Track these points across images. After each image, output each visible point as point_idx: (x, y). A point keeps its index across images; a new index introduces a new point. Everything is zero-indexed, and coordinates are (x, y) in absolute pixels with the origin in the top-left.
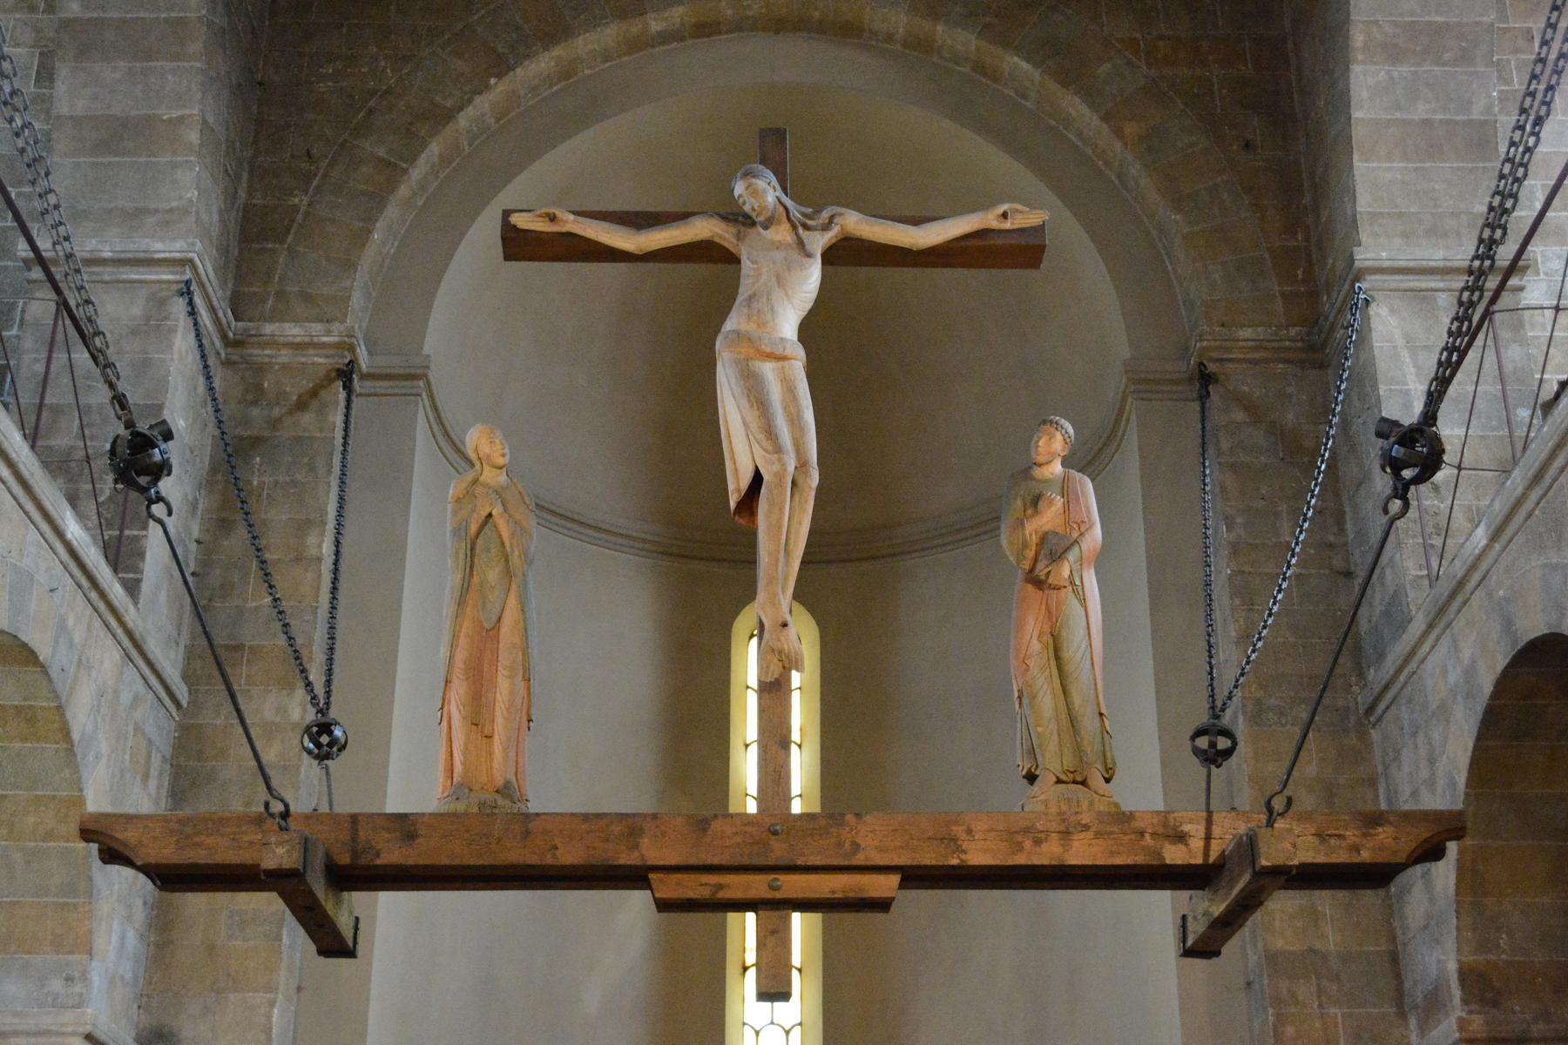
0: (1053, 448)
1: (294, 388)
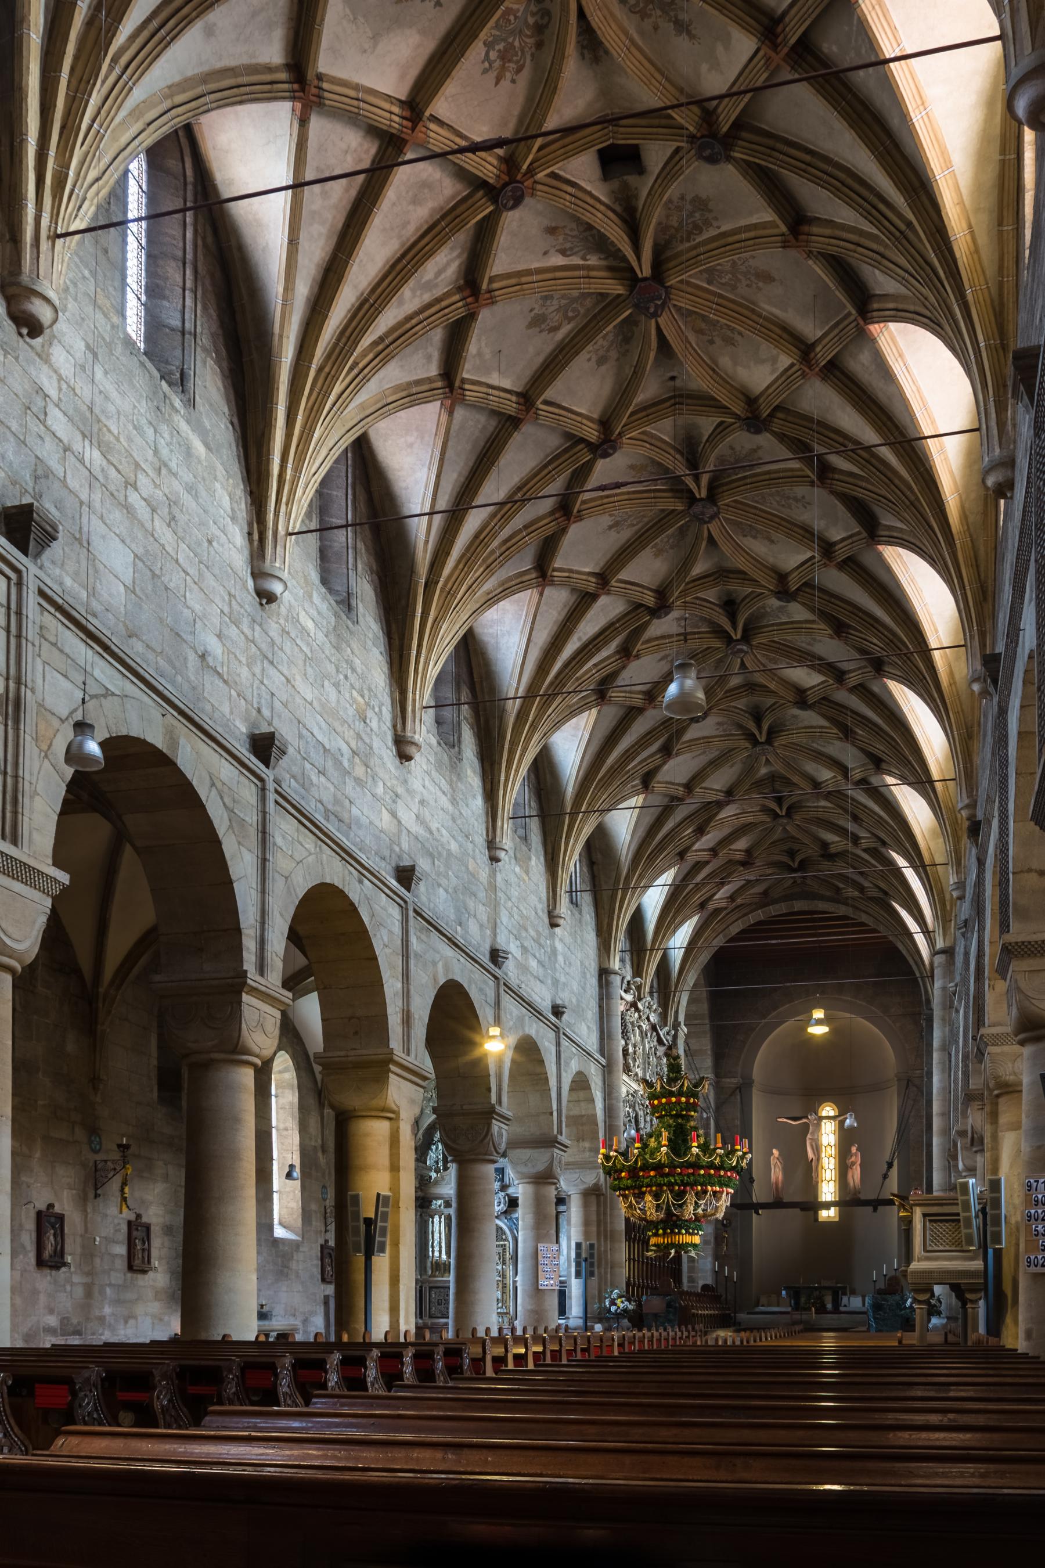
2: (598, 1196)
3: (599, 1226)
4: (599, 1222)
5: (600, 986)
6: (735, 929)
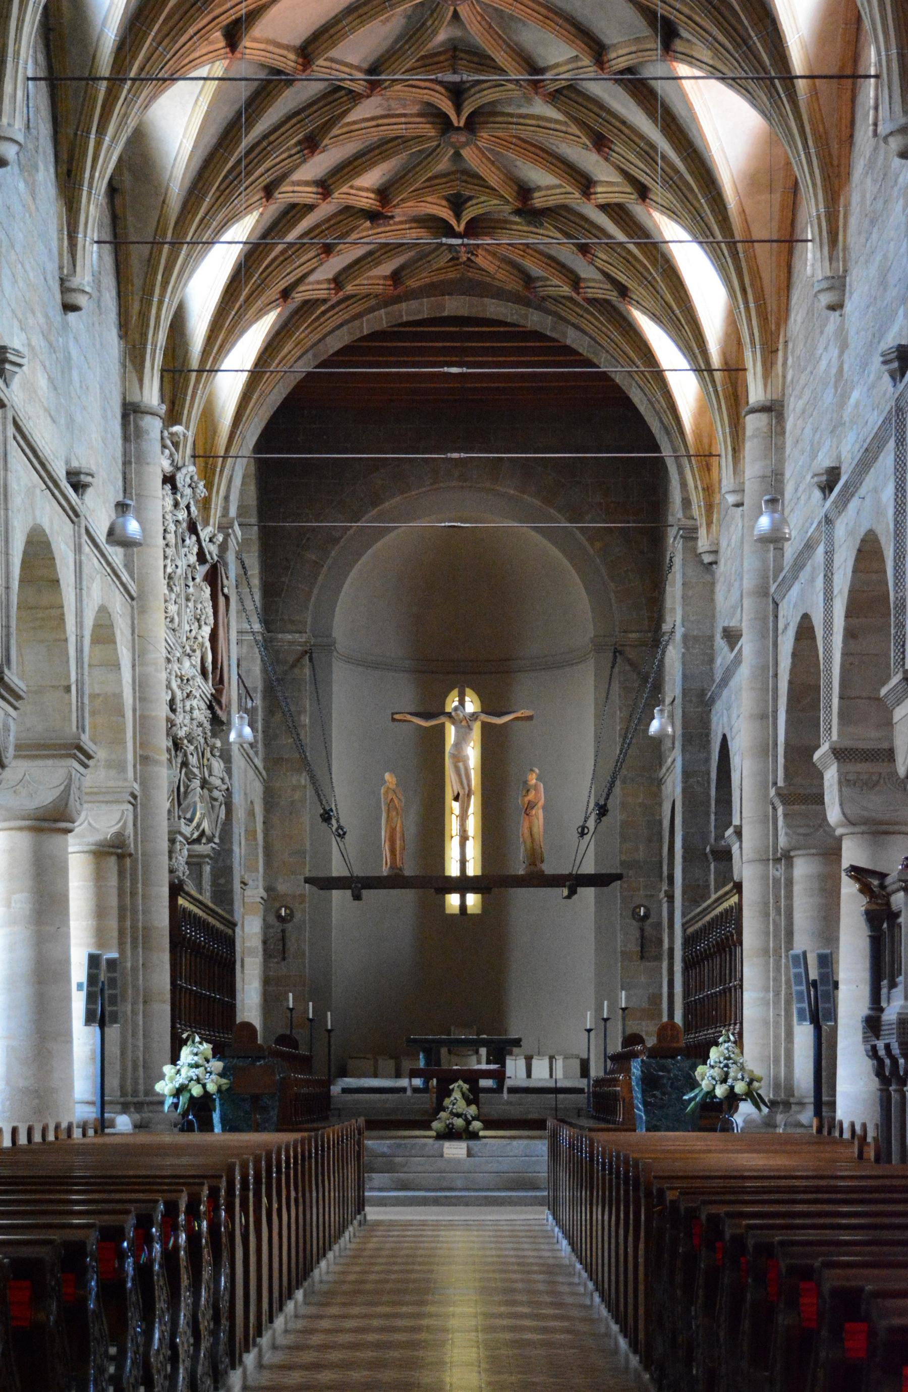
0: (533, 779)
1: (291, 659)
2: (121, 857)
3: (122, 918)
4: (122, 909)
5: (126, 438)
6: (335, 344)
